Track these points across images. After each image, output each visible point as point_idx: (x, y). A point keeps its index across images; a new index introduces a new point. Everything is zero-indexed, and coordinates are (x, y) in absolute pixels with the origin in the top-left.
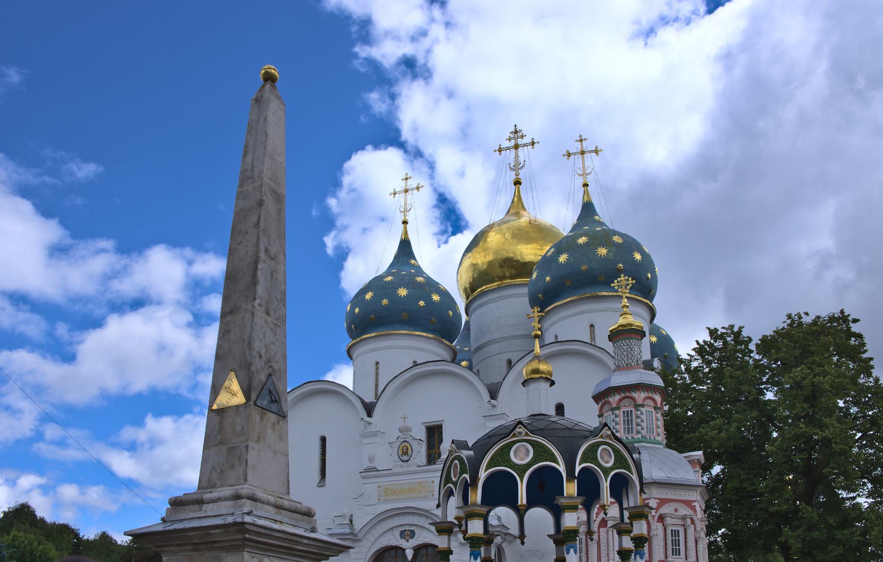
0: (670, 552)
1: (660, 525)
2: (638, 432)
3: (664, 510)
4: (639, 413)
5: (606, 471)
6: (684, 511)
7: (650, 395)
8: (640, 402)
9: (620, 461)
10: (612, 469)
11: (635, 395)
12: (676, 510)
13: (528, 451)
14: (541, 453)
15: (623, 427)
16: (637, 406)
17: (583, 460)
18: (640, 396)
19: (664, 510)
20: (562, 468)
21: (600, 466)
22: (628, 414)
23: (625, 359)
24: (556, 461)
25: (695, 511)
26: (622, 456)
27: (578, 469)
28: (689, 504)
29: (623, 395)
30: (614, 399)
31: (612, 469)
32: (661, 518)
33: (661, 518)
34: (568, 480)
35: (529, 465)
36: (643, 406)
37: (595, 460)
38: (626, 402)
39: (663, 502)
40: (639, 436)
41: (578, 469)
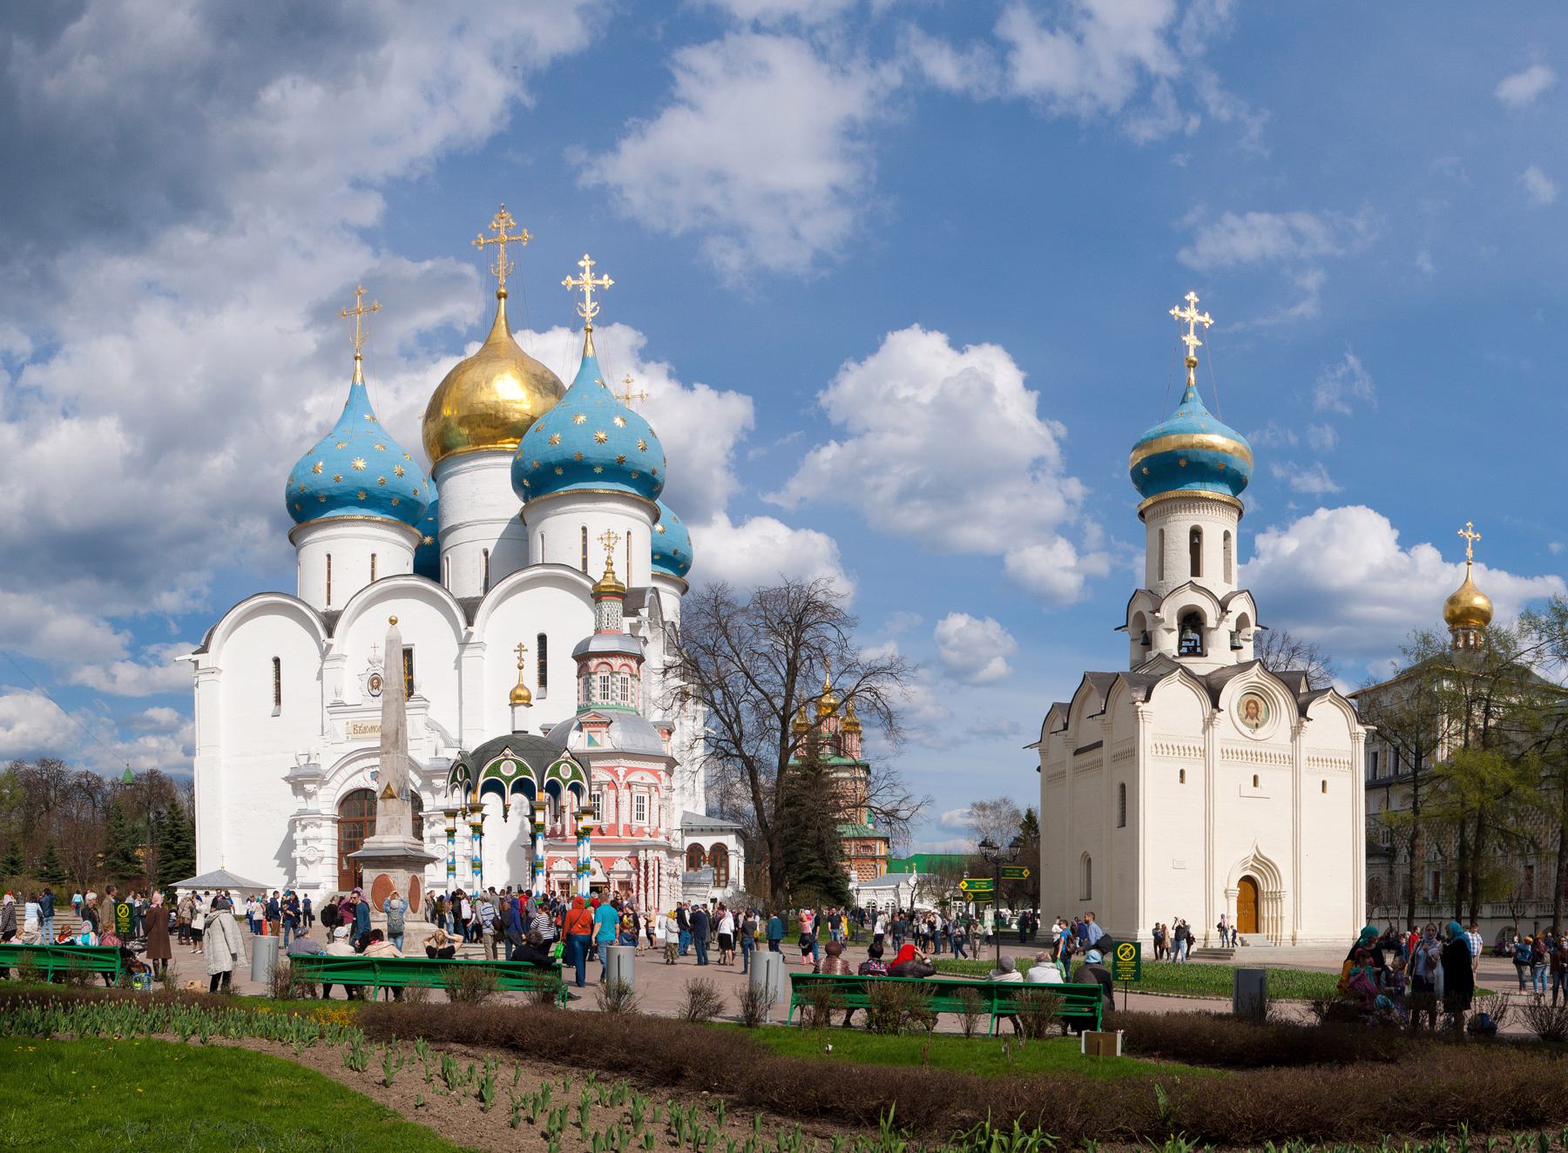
0: (634, 817)
1: (627, 792)
2: (612, 699)
3: (632, 778)
4: (614, 680)
5: (565, 782)
6: (650, 779)
7: (627, 661)
8: (616, 669)
9: (576, 774)
10: (569, 780)
11: (612, 661)
12: (642, 778)
13: (512, 767)
14: (521, 768)
15: (599, 692)
16: (612, 673)
17: (549, 776)
18: (616, 663)
19: (632, 778)
20: (535, 781)
21: (561, 778)
22: (605, 679)
23: (606, 622)
24: (531, 775)
25: (660, 780)
26: (578, 771)
27: (546, 781)
28: (654, 772)
29: (600, 660)
30: (594, 663)
31: (569, 780)
32: (629, 786)
33: (629, 786)
34: (539, 791)
35: (513, 777)
36: (618, 673)
37: (558, 775)
38: (604, 667)
39: (630, 771)
40: (614, 703)
41: (546, 781)
